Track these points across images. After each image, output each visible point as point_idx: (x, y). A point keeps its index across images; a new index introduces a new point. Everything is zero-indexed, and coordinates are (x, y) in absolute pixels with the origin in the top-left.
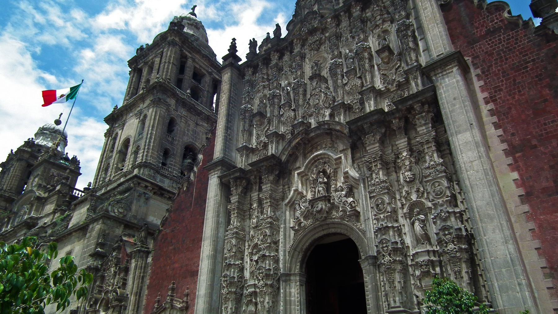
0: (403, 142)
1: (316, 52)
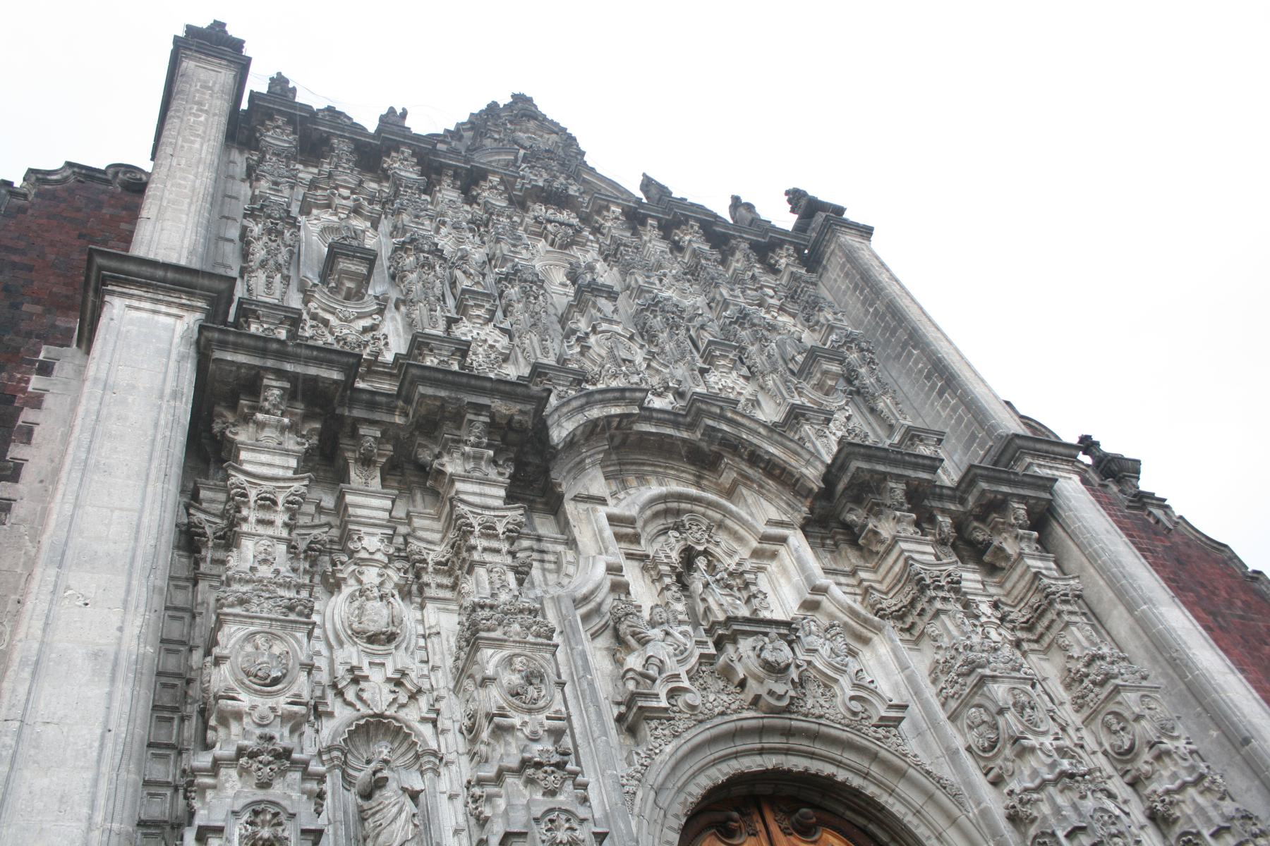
0: (971, 581)
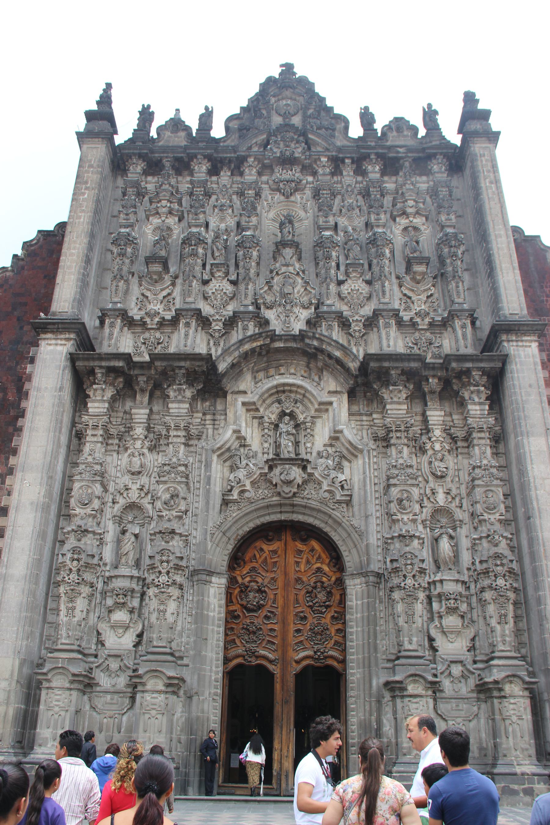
1: (282, 198)
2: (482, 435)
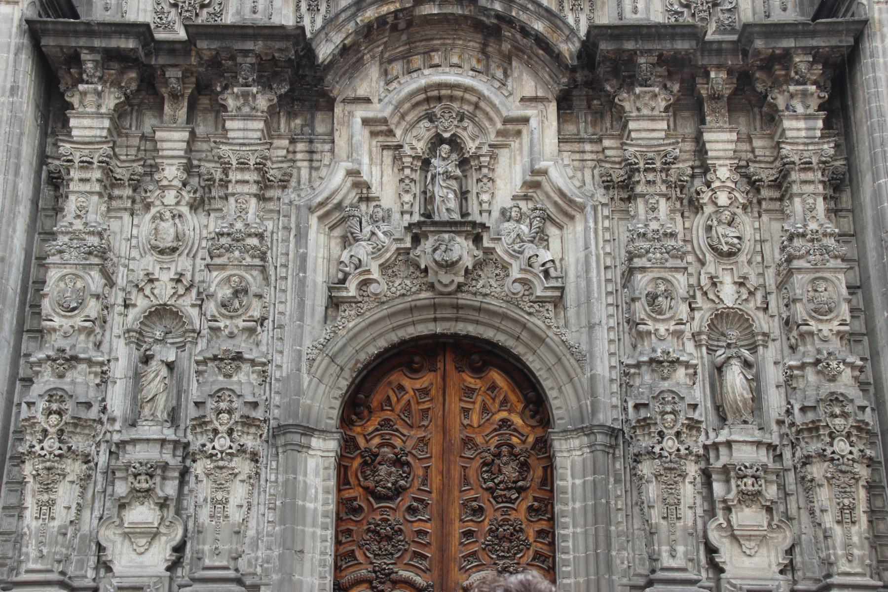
2: (809, 176)
